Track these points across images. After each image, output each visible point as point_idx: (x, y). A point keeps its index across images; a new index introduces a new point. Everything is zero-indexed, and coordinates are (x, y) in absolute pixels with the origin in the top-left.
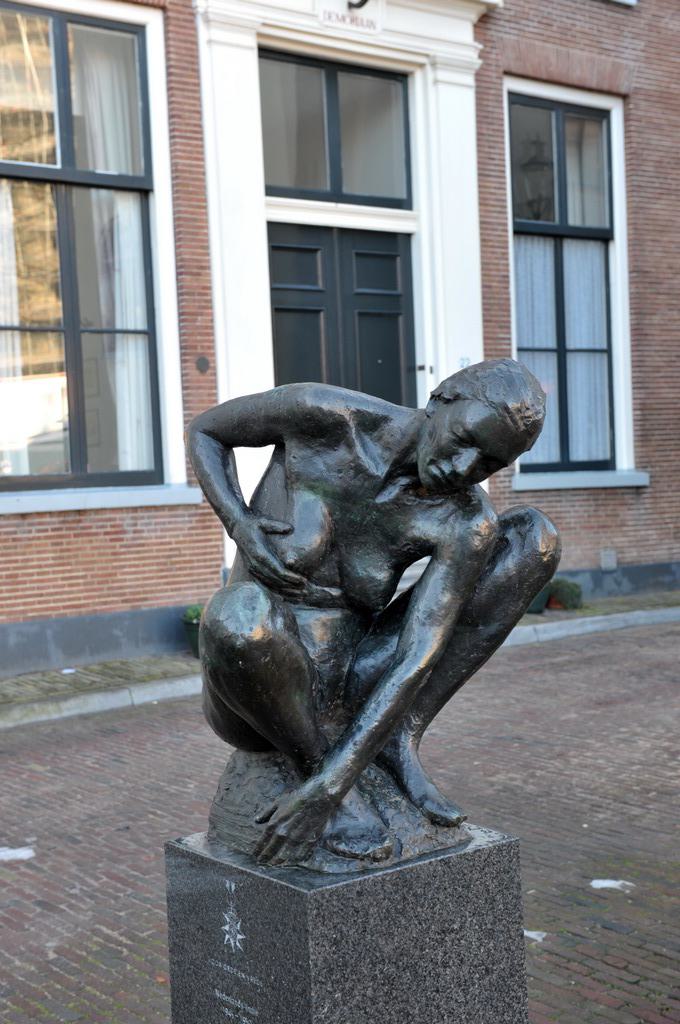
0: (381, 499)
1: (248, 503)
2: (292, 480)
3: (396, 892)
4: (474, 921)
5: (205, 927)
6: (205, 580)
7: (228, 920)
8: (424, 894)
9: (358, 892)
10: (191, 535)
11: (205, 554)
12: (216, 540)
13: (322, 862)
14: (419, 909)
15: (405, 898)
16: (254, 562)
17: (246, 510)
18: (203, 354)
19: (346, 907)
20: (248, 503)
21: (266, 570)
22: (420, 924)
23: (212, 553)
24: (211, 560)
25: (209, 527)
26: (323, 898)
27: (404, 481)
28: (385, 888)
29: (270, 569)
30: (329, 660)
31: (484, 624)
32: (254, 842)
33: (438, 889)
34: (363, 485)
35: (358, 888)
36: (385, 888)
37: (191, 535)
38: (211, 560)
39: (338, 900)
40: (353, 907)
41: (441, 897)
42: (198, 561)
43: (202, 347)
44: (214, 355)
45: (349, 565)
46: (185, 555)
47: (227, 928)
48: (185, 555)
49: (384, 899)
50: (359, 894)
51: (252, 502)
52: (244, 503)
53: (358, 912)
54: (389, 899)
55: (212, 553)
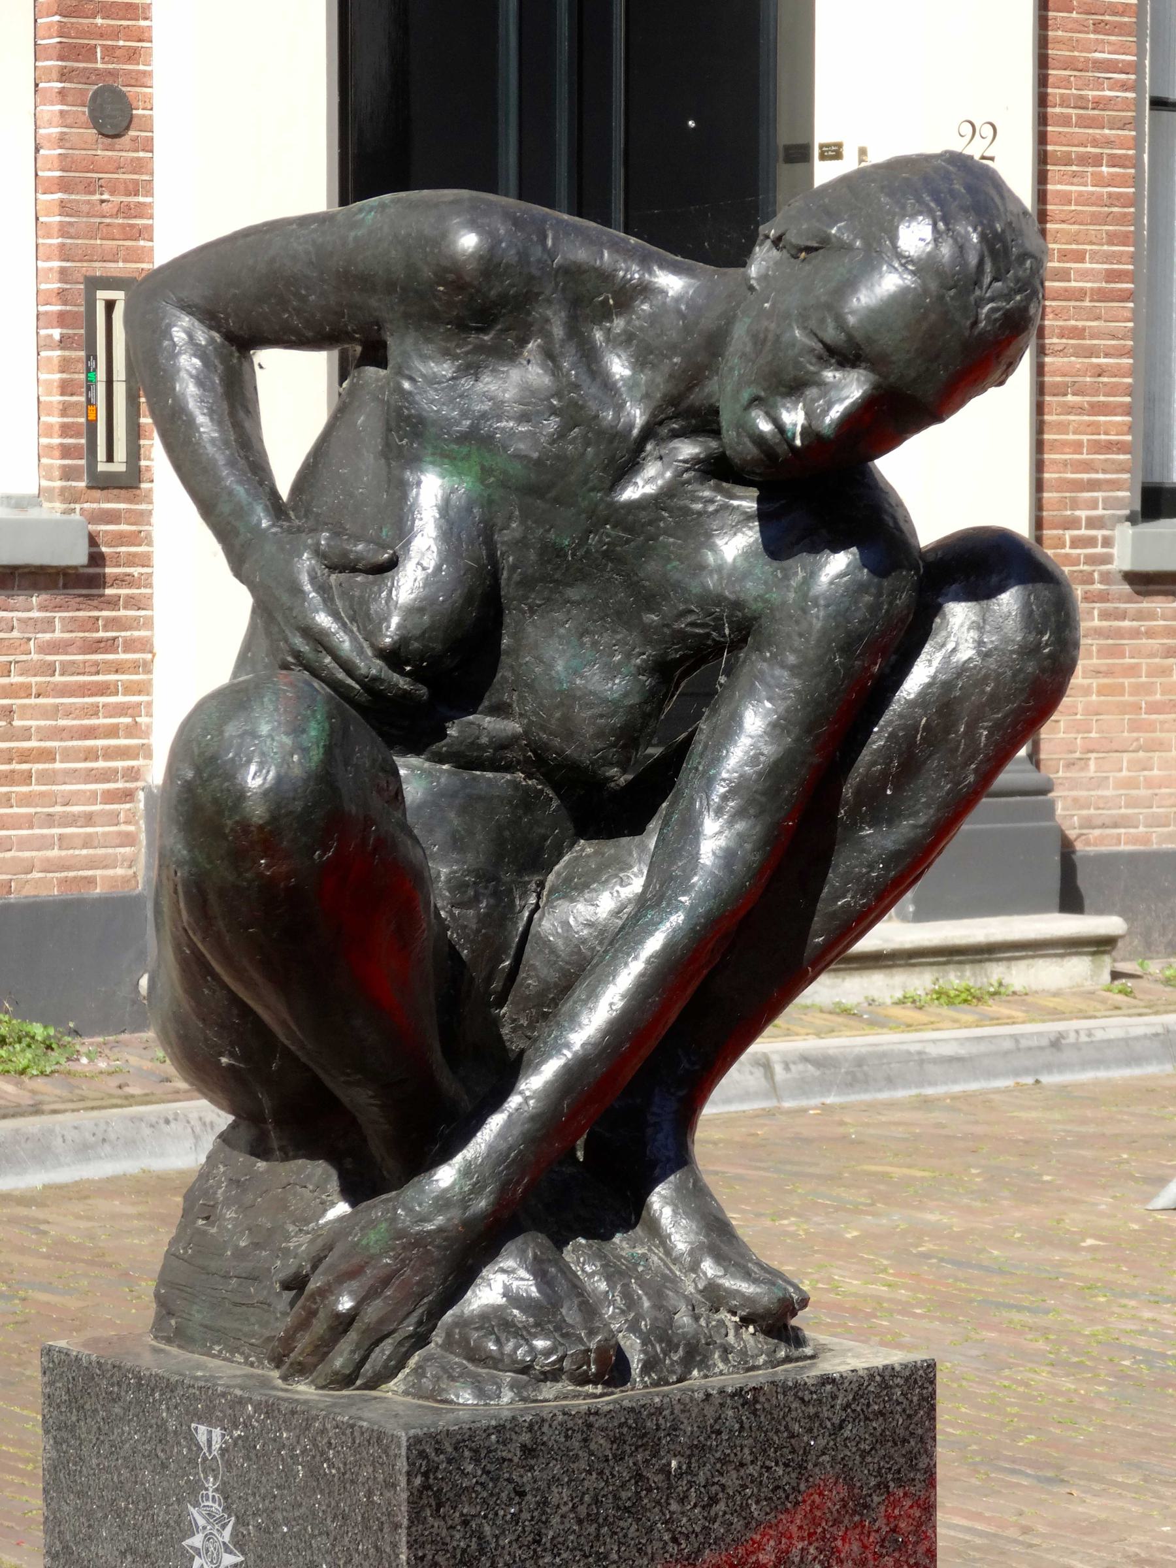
0: (633, 492)
1: (284, 490)
2: (409, 437)
3: (619, 1458)
4: (812, 1550)
5: (141, 1548)
6: (89, 820)
7: (201, 1522)
8: (689, 1471)
9: (524, 1447)
10: (50, 669)
11: (90, 733)
12: (129, 689)
13: (438, 1378)
14: (674, 1506)
15: (639, 1477)
16: (299, 642)
17: (277, 508)
18: (113, 74)
19: (495, 1480)
20: (284, 490)
21: (328, 660)
22: (675, 1540)
23: (113, 732)
24: (109, 754)
25: (109, 645)
26: (438, 1451)
27: (688, 450)
28: (593, 1446)
29: (336, 658)
30: (476, 899)
31: (875, 822)
32: (270, 1339)
33: (724, 1461)
34: (583, 454)
35: (525, 1438)
36: (593, 1446)
37: (50, 669)
38: (109, 754)
39: (476, 1460)
40: (510, 1480)
41: (731, 1480)
42: (67, 755)
43: (109, 52)
44: (142, 80)
45: (540, 660)
46: (26, 734)
47: (197, 1541)
48: (26, 734)
49: (589, 1473)
50: (528, 1451)
51: (303, 482)
52: (274, 494)
53: (522, 1494)
54: (601, 1473)
55: (113, 732)
